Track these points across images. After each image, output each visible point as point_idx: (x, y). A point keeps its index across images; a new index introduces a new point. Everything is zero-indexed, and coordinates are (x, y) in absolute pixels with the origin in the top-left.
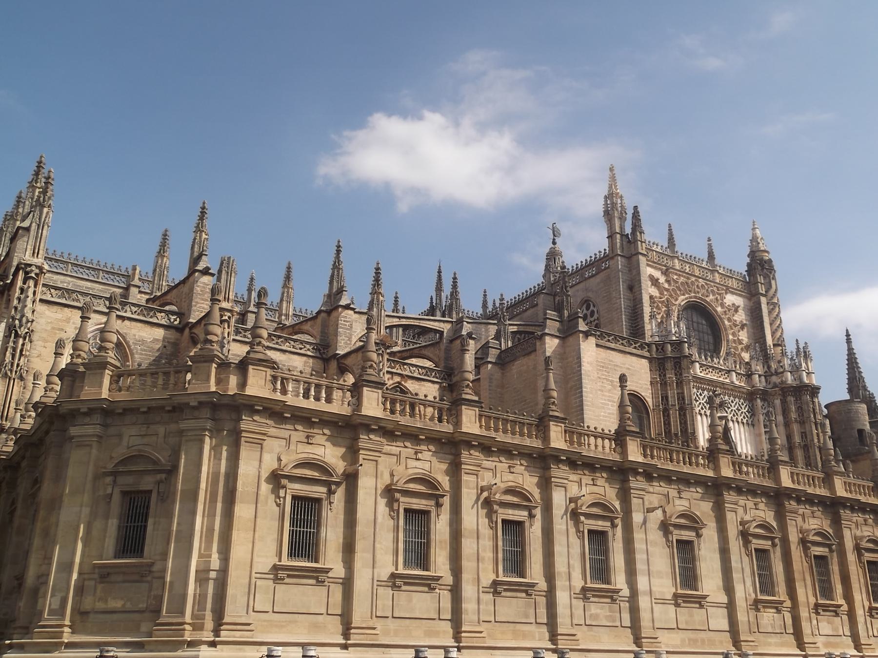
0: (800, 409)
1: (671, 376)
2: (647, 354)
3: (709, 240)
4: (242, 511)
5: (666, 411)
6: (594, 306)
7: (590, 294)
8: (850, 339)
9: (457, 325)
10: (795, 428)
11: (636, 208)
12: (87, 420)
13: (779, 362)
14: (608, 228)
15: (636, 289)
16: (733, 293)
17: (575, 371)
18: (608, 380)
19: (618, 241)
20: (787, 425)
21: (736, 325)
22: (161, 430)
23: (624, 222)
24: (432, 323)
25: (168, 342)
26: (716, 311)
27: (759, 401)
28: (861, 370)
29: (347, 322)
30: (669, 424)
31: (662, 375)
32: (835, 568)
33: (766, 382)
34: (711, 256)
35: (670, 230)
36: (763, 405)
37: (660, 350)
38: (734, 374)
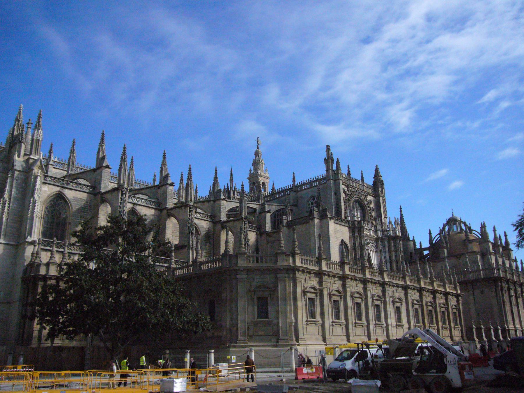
0: (395, 246)
1: (357, 235)
2: (348, 225)
3: (362, 172)
4: (299, 304)
5: (355, 249)
10: (393, 254)
11: (338, 159)
12: (242, 273)
13: (388, 226)
15: (338, 194)
16: (370, 195)
18: (336, 237)
19: (331, 173)
20: (390, 252)
21: (371, 209)
22: (268, 277)
24: (252, 205)
25: (156, 216)
26: (364, 203)
27: (380, 242)
28: (405, 224)
30: (356, 254)
32: (434, 314)
34: (362, 179)
38: (371, 230)
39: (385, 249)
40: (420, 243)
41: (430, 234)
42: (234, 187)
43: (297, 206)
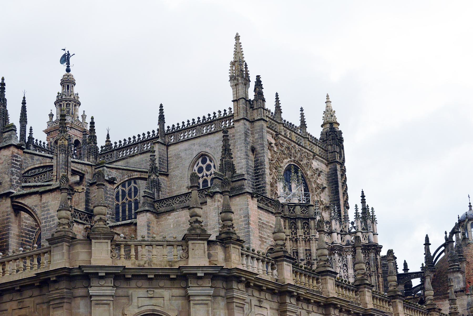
6: (211, 161)
7: (208, 150)
8: (365, 200)
9: (95, 169)
11: (258, 77)
13: (353, 223)
14: (233, 92)
17: (241, 228)
22: (166, 293)
23: (248, 89)
27: (336, 255)
29: (18, 161)
31: (293, 233)
33: (342, 238)
35: (277, 98)
36: (339, 259)
37: (292, 211)
39: (347, 271)
40: (405, 264)
41: (427, 244)
42: (27, 135)
43: (167, 175)
